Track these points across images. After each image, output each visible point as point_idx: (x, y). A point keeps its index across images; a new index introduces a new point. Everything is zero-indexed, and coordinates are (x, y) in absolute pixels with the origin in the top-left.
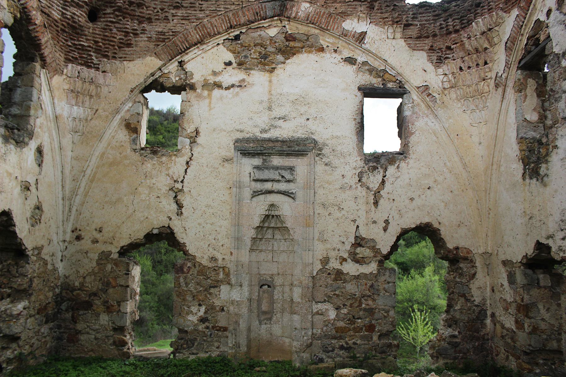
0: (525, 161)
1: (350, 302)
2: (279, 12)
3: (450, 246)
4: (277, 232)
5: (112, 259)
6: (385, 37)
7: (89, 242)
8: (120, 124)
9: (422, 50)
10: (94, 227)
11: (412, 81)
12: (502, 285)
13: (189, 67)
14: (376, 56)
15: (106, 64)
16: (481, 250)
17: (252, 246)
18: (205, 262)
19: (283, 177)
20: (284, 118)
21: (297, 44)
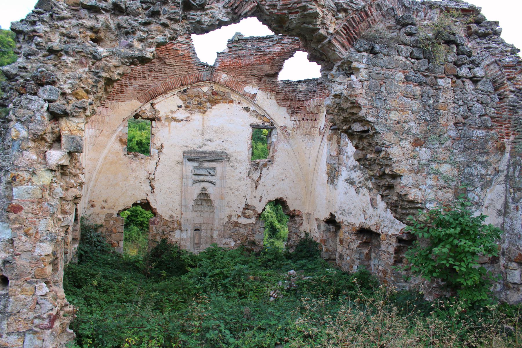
0: (329, 175)
1: (242, 237)
2: (209, 78)
3: (291, 209)
4: (204, 201)
5: (113, 218)
6: (266, 97)
7: (99, 208)
8: (116, 139)
9: (285, 106)
10: (102, 200)
11: (278, 123)
12: (315, 230)
13: (157, 107)
14: (260, 108)
15: (109, 103)
16: (306, 212)
17: (193, 209)
18: (167, 218)
19: (209, 173)
20: (210, 140)
21: (219, 98)
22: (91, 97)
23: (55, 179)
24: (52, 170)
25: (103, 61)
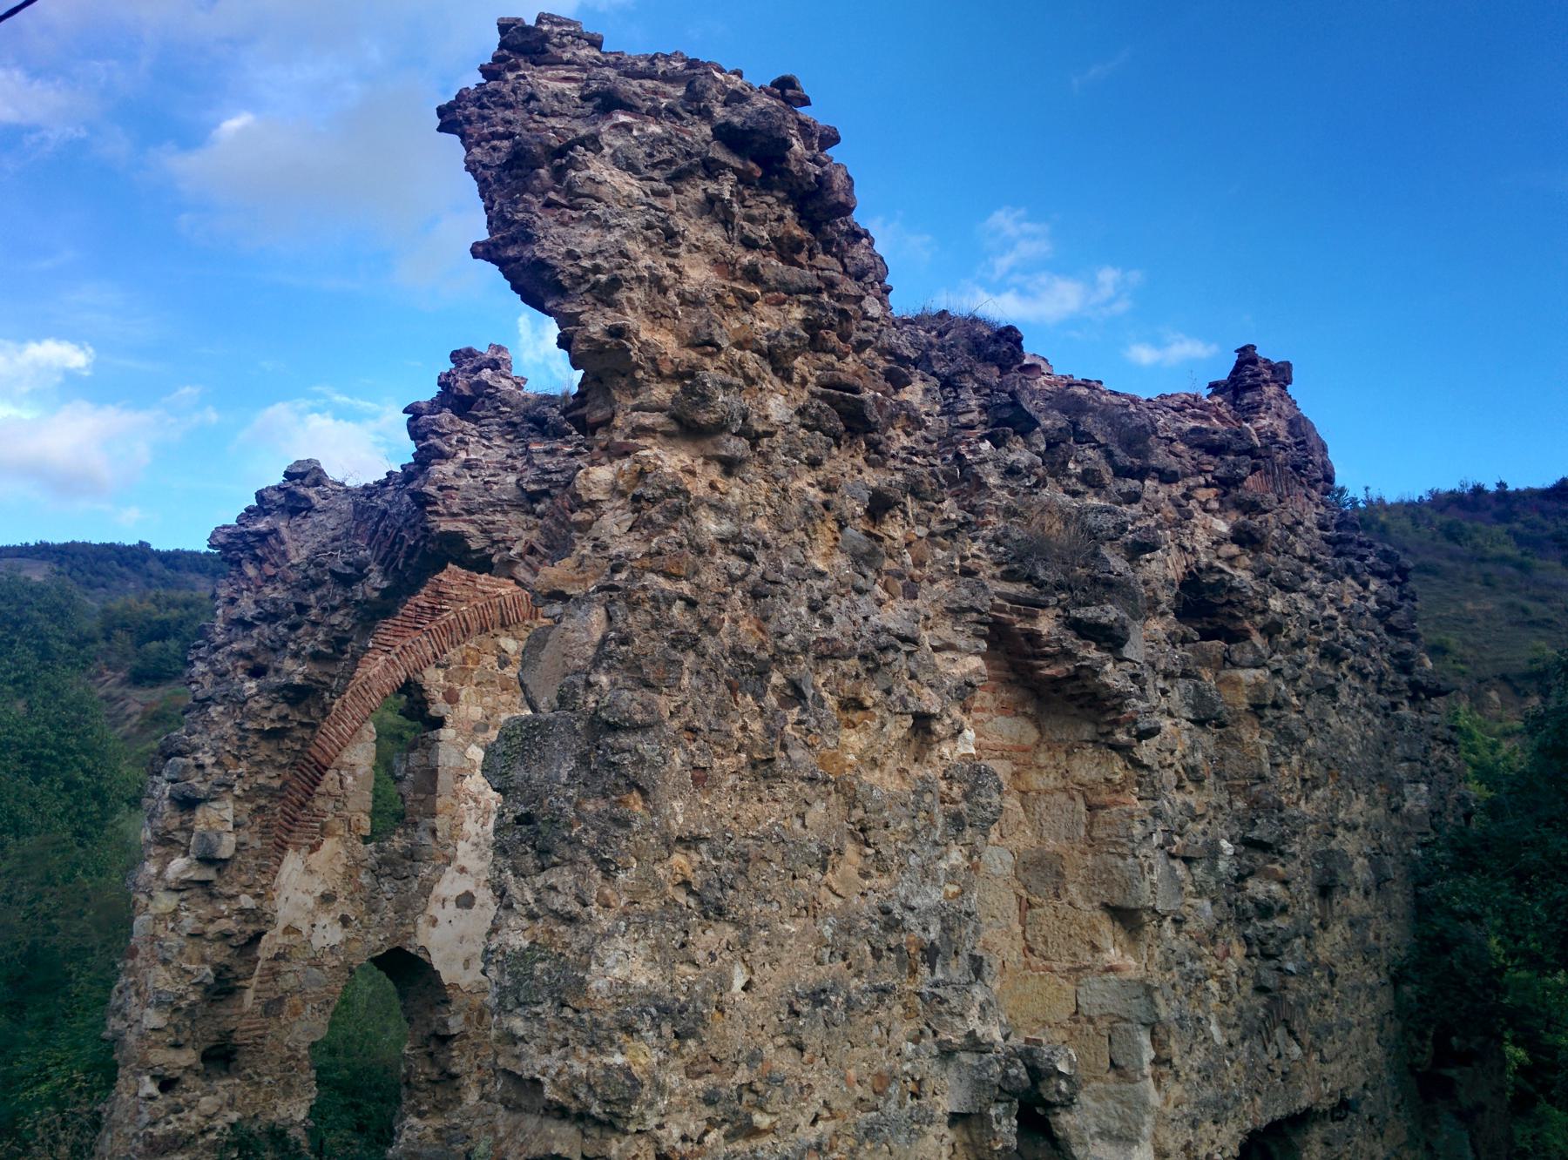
22: (244, 763)
23: (183, 904)
24: (178, 891)
25: (251, 704)
